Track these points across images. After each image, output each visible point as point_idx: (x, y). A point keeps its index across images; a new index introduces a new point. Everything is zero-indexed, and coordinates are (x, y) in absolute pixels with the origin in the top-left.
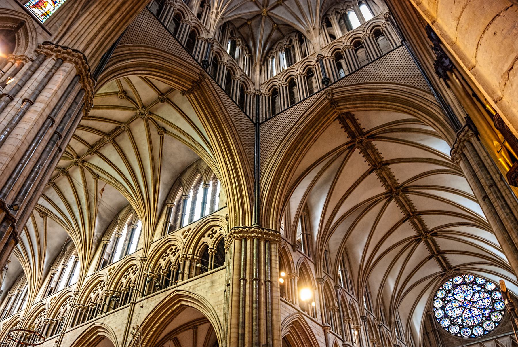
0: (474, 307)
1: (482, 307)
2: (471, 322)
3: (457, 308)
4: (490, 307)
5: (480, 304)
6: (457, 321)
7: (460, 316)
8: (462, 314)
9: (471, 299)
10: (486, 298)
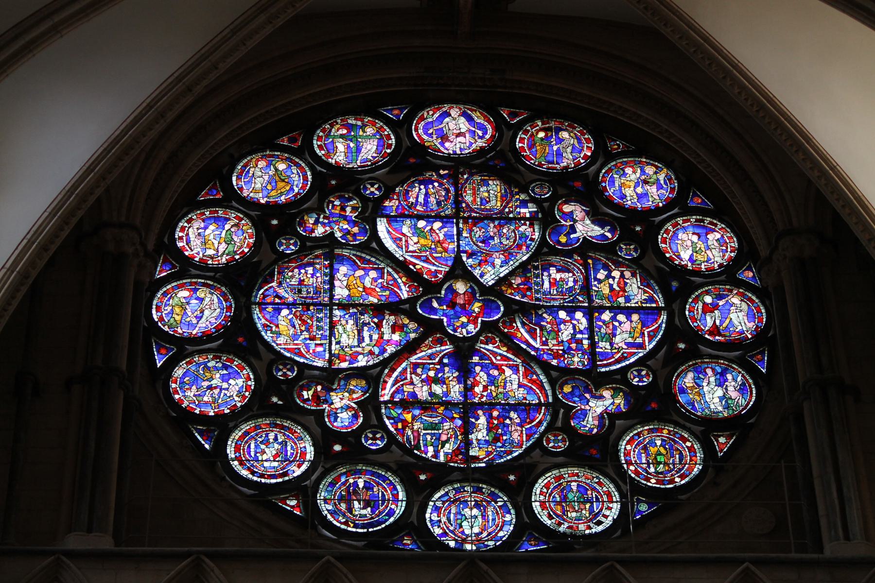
0: (509, 341)
1: (577, 361)
3: (365, 308)
4: (640, 380)
5: (566, 333)
6: (316, 398)
8: (384, 363)
10: (628, 312)
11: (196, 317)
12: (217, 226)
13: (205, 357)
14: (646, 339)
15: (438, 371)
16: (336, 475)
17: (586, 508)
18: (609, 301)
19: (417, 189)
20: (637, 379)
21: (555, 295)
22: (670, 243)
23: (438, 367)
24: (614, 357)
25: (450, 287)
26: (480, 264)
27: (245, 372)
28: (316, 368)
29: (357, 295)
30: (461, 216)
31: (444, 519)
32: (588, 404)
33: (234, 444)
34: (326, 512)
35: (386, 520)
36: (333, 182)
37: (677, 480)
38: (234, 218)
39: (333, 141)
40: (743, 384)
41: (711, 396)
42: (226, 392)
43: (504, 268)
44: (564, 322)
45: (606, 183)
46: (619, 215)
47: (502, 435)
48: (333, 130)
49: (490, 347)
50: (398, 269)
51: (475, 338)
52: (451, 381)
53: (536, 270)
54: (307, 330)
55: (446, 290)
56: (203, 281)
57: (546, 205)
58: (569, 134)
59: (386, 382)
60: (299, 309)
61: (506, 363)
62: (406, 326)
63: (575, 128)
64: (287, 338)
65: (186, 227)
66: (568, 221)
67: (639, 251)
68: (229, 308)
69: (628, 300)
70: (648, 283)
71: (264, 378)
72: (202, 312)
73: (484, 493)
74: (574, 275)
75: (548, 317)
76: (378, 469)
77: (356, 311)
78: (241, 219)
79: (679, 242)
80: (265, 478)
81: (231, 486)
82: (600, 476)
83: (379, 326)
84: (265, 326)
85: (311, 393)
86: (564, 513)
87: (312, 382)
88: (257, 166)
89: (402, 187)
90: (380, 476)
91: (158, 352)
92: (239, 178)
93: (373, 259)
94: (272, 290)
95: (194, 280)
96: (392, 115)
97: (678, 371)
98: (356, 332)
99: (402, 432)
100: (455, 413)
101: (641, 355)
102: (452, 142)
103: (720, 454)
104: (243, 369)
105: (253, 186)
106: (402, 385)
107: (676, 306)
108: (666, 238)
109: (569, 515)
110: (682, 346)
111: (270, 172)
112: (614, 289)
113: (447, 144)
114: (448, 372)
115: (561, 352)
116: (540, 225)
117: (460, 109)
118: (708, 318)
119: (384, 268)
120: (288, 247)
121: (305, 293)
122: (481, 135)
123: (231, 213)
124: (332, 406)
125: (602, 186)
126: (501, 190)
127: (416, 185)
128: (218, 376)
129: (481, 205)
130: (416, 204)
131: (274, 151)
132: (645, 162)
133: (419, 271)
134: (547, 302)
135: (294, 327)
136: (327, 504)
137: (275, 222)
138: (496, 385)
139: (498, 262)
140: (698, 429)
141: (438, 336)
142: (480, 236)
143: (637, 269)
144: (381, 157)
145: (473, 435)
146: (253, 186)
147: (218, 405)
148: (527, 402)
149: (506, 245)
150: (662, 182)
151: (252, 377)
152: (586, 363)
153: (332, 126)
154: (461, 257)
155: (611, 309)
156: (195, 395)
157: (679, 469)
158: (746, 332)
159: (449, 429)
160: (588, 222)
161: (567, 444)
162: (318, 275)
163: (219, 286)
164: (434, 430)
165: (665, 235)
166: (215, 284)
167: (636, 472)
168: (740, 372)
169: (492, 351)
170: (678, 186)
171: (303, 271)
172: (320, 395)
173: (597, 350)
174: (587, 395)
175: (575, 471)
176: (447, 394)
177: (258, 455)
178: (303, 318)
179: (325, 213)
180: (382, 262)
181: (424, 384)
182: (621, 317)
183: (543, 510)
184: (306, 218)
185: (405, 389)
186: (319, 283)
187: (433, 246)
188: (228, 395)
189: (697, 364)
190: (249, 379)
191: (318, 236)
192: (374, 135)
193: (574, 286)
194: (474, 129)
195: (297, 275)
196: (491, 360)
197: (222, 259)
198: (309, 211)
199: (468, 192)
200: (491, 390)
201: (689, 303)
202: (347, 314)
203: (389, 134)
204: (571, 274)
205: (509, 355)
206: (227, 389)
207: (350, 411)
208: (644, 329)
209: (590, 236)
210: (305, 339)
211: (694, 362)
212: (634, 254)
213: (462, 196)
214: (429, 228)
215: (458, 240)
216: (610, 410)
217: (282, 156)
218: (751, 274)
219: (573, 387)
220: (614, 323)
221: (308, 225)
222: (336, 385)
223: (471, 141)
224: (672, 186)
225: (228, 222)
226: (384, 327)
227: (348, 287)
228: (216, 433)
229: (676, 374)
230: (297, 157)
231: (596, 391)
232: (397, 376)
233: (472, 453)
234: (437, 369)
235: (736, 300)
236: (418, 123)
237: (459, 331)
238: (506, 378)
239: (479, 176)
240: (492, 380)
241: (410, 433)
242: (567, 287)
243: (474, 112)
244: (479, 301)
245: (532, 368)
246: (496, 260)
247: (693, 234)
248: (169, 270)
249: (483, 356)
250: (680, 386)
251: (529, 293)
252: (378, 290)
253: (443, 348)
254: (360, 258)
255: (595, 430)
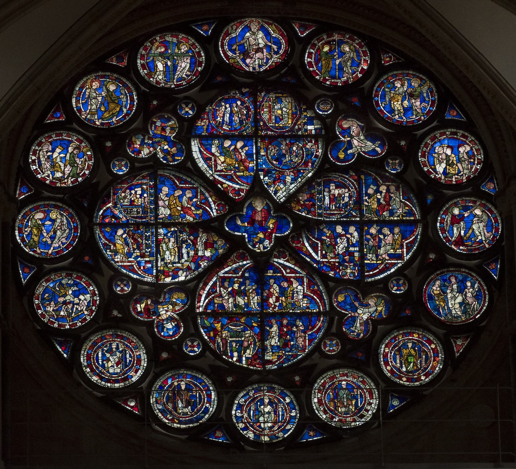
2: (241, 349)
3: (182, 226)
5: (341, 248)
7: (181, 287)
9: (292, 197)
10: (391, 225)
11: (51, 238)
12: (62, 149)
13: (59, 275)
14: (405, 250)
15: (241, 284)
16: (165, 378)
17: (352, 404)
18: (376, 215)
19: (224, 107)
20: (395, 288)
21: (334, 210)
22: (428, 157)
23: (242, 280)
24: (378, 268)
25: (251, 204)
26: (274, 183)
27: (91, 288)
28: (147, 283)
29: (177, 214)
30: (259, 134)
31: (246, 415)
32: (356, 311)
33: (86, 353)
34: (157, 411)
35: (203, 417)
36: (155, 103)
37: (423, 378)
38: (75, 140)
39: (153, 59)
40: (479, 290)
41: (453, 302)
42: (78, 307)
43: (293, 185)
44: (340, 236)
45: (378, 98)
46: (388, 130)
47: (290, 341)
48: (154, 47)
49: (281, 261)
50: (209, 188)
51: (269, 254)
52: (251, 293)
53: (319, 187)
54: (139, 248)
55: (247, 208)
56: (54, 203)
57: (328, 121)
58: (350, 47)
59: (201, 296)
60: (131, 229)
61: (294, 275)
62: (216, 242)
63: (354, 40)
64: (122, 256)
65: (37, 150)
66: (346, 136)
67: (403, 165)
68: (76, 228)
69: (392, 213)
70: (408, 197)
71: (106, 293)
72: (55, 232)
73: (276, 393)
74: (349, 190)
75: (328, 232)
76: (196, 373)
77: (176, 229)
78: (81, 142)
79: (436, 155)
80: (110, 383)
81: (86, 389)
82: (364, 376)
83: (195, 243)
84: (105, 245)
85: (143, 306)
86: (335, 409)
87: (144, 296)
88: (92, 87)
89: (211, 106)
90: (197, 379)
91: (23, 271)
92: (77, 101)
93: (189, 179)
94: (109, 211)
95: (46, 203)
96: (202, 30)
97: (429, 280)
98: (176, 249)
99: (213, 340)
100: (254, 322)
101: (399, 265)
102: (252, 58)
103: (457, 355)
104: (89, 285)
105: (89, 108)
106: (213, 297)
107: (429, 218)
108: (425, 152)
109: (340, 410)
110: (432, 256)
111: (103, 93)
112: (381, 203)
113: (248, 61)
114: (249, 285)
115: (337, 264)
116: (323, 142)
117: (259, 23)
118: (455, 229)
119: (197, 188)
120: (120, 169)
121: (135, 213)
122: (276, 50)
123: (73, 136)
124: (160, 318)
125: (375, 100)
126: (292, 108)
127: (223, 104)
128: (70, 292)
129: (275, 123)
130: (223, 124)
131: (105, 72)
132: (412, 74)
133: (226, 190)
134: (327, 218)
135: (127, 245)
136: (158, 404)
137: (109, 144)
138: (286, 296)
139: (288, 179)
140: (441, 332)
141: (241, 251)
142: (274, 154)
143: (400, 183)
144: (194, 75)
145: (268, 342)
146: (89, 108)
147: (72, 318)
148: (310, 311)
149: (295, 163)
150: (425, 95)
151: (97, 292)
152: (356, 274)
153: (152, 43)
154: (259, 175)
155: (377, 222)
156: (53, 310)
157: (424, 368)
158: (484, 242)
159: (250, 336)
160: (362, 138)
161: (340, 348)
162: (145, 195)
163: (67, 208)
164: (238, 337)
165: (425, 149)
166: (64, 206)
167: (392, 372)
168: (477, 280)
169: (283, 264)
170: (438, 99)
171: (133, 192)
172: (151, 308)
173: (366, 262)
174: (357, 304)
175: (345, 372)
176: (247, 305)
177: (105, 362)
178: (135, 237)
179: (150, 134)
180: (196, 182)
181: (230, 296)
182: (386, 231)
183: (320, 406)
184: (133, 139)
185: (216, 301)
186: (147, 203)
187: (237, 165)
188: (79, 309)
189: (443, 272)
190: (94, 294)
191: (144, 157)
192: (187, 52)
193: (349, 201)
194: (270, 44)
195: (129, 196)
196: (282, 273)
197: (68, 181)
198: (136, 132)
199: (265, 110)
200: (282, 300)
201: (440, 215)
202: (169, 232)
203: (200, 52)
204: (347, 190)
205: (296, 268)
206: (78, 304)
207: (174, 322)
208: (403, 241)
209: (364, 152)
210: (137, 257)
211: (441, 271)
212: (398, 168)
213: (260, 115)
214: (233, 147)
215: (257, 159)
216: (373, 317)
217: (112, 76)
218: (492, 186)
219: (345, 297)
220: (380, 236)
221: (135, 146)
222: (162, 299)
223: (268, 57)
224: (433, 98)
225: (71, 145)
226: (198, 244)
227: (169, 207)
228: (72, 344)
229: (427, 282)
230: (124, 77)
231: (363, 299)
232: (209, 290)
233: (268, 357)
234: (240, 282)
235: (478, 212)
236: (224, 39)
237: (257, 246)
238: (294, 289)
239: (274, 93)
240: (283, 292)
241: (219, 341)
242: (343, 202)
243: (270, 26)
244: (273, 218)
245: (314, 279)
246: (287, 177)
247: (448, 147)
248: (26, 193)
249: (276, 270)
250: (429, 293)
251: (312, 209)
252: (193, 208)
253: (245, 263)
254: (179, 179)
255: (362, 335)
